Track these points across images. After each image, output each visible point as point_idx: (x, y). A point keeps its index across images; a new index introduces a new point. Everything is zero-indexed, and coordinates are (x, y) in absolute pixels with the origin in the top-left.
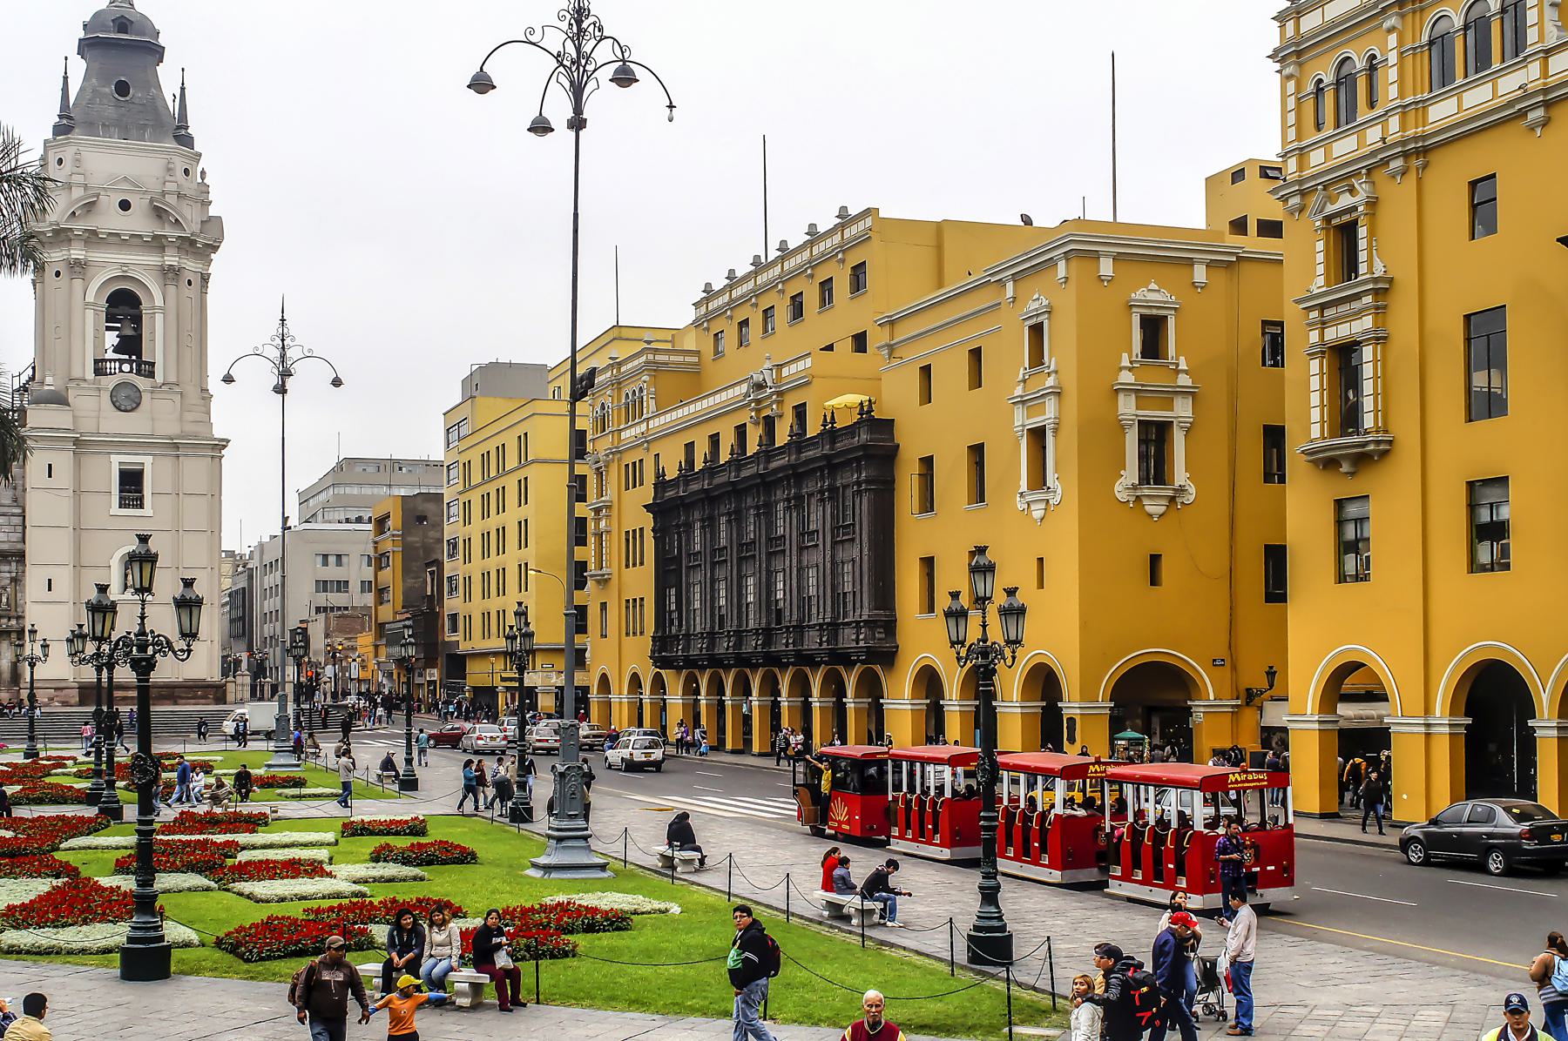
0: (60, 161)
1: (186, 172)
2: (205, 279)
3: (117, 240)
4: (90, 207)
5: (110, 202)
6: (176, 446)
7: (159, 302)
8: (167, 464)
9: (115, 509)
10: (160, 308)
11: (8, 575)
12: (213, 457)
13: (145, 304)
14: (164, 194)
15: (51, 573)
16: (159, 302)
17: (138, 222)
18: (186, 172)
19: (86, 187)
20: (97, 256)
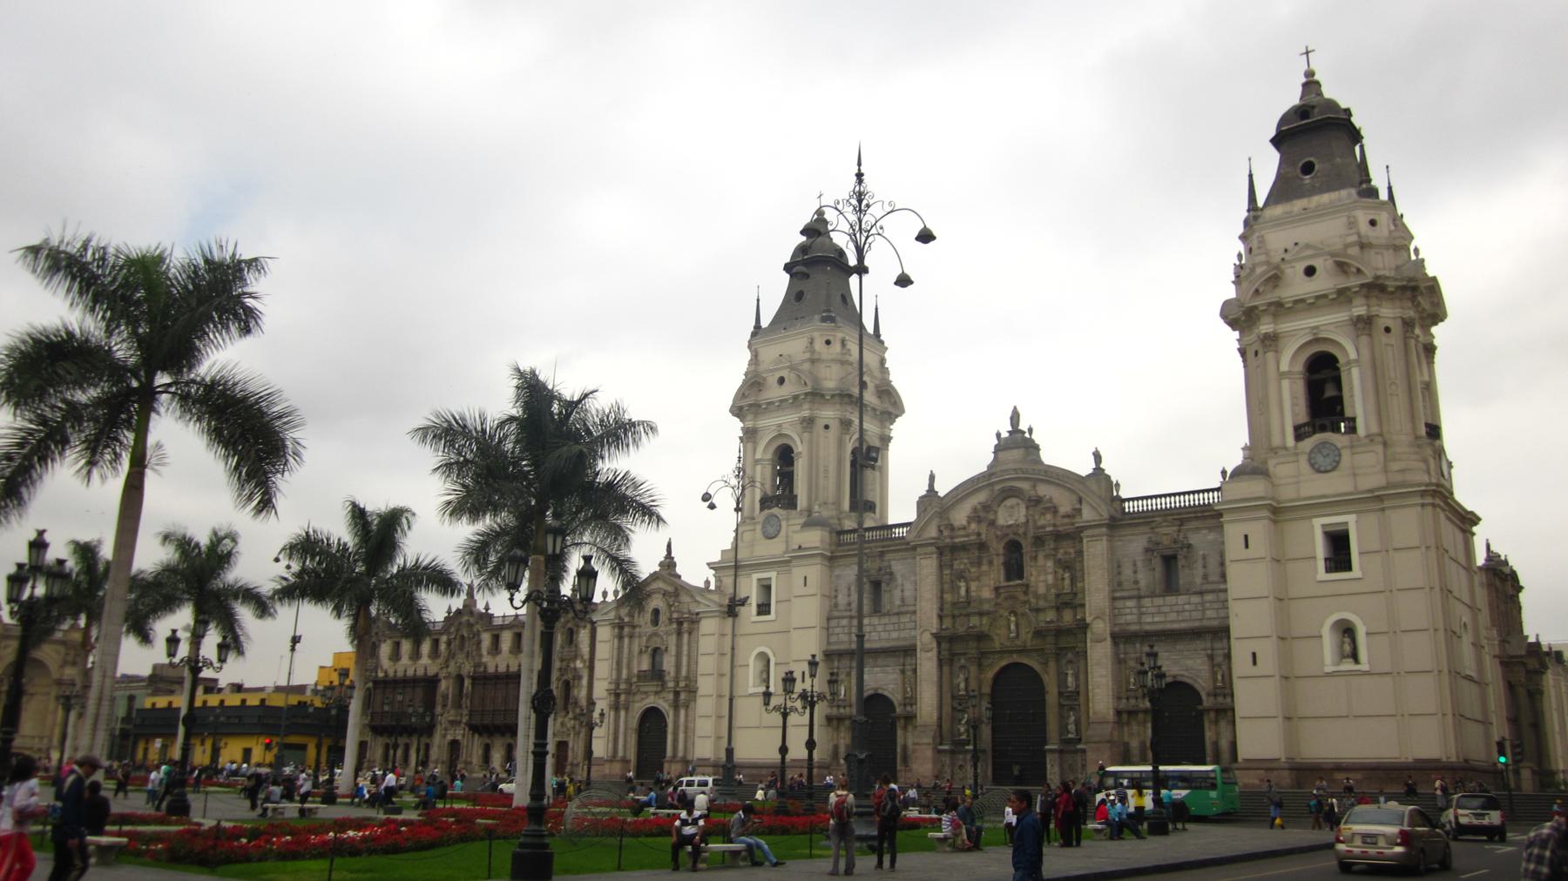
1: (1373, 223)
4: (1275, 279)
5: (1295, 271)
6: (1380, 498)
7: (1353, 355)
8: (1372, 519)
10: (1356, 361)
11: (1220, 652)
12: (1423, 505)
13: (1342, 360)
14: (1347, 246)
16: (1353, 355)
17: (1325, 282)
18: (1373, 223)
19: (1268, 263)
20: (1286, 326)
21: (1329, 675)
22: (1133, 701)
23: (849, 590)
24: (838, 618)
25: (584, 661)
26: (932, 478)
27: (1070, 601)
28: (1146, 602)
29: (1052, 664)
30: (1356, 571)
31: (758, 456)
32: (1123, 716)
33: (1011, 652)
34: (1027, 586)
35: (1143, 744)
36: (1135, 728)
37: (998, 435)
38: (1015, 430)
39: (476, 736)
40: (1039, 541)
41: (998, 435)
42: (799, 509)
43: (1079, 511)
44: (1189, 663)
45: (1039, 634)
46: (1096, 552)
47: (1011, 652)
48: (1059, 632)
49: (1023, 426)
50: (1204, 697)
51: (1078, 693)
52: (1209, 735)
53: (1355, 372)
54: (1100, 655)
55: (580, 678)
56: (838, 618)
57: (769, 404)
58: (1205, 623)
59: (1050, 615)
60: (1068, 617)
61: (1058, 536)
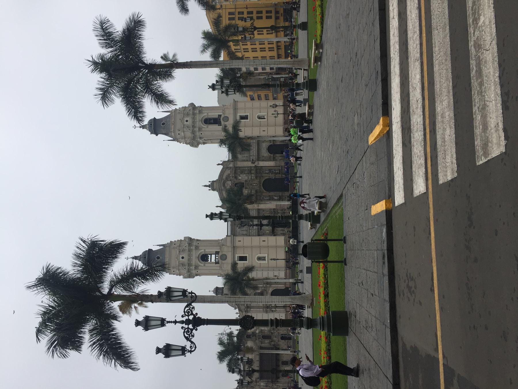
0: (179, 134)
2: (201, 107)
3: (194, 122)
9: (248, 120)
13: (206, 117)
15: (261, 131)
21: (267, 120)
22: (271, 158)
23: (242, 230)
24: (249, 233)
25: (256, 330)
26: (217, 207)
27: (250, 171)
28: (251, 154)
29: (263, 175)
30: (248, 114)
31: (203, 265)
32: (274, 159)
33: (260, 185)
34: (246, 181)
35: (280, 156)
36: (277, 158)
37: (210, 190)
38: (209, 186)
39: (279, 380)
40: (236, 178)
41: (210, 190)
42: (219, 250)
43: (230, 168)
44: (264, 146)
45: (256, 177)
46: (240, 164)
47: (260, 185)
48: (256, 172)
49: (208, 183)
50: (271, 144)
51: (269, 169)
52: (278, 143)
53: (209, 114)
54: (262, 164)
55: (262, 330)
56: (249, 233)
57: (189, 261)
58: (256, 142)
59: (253, 175)
60: (253, 172)
61: (235, 173)
